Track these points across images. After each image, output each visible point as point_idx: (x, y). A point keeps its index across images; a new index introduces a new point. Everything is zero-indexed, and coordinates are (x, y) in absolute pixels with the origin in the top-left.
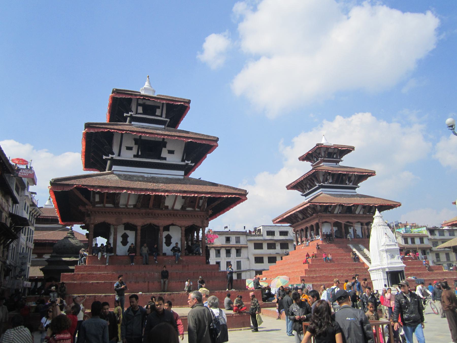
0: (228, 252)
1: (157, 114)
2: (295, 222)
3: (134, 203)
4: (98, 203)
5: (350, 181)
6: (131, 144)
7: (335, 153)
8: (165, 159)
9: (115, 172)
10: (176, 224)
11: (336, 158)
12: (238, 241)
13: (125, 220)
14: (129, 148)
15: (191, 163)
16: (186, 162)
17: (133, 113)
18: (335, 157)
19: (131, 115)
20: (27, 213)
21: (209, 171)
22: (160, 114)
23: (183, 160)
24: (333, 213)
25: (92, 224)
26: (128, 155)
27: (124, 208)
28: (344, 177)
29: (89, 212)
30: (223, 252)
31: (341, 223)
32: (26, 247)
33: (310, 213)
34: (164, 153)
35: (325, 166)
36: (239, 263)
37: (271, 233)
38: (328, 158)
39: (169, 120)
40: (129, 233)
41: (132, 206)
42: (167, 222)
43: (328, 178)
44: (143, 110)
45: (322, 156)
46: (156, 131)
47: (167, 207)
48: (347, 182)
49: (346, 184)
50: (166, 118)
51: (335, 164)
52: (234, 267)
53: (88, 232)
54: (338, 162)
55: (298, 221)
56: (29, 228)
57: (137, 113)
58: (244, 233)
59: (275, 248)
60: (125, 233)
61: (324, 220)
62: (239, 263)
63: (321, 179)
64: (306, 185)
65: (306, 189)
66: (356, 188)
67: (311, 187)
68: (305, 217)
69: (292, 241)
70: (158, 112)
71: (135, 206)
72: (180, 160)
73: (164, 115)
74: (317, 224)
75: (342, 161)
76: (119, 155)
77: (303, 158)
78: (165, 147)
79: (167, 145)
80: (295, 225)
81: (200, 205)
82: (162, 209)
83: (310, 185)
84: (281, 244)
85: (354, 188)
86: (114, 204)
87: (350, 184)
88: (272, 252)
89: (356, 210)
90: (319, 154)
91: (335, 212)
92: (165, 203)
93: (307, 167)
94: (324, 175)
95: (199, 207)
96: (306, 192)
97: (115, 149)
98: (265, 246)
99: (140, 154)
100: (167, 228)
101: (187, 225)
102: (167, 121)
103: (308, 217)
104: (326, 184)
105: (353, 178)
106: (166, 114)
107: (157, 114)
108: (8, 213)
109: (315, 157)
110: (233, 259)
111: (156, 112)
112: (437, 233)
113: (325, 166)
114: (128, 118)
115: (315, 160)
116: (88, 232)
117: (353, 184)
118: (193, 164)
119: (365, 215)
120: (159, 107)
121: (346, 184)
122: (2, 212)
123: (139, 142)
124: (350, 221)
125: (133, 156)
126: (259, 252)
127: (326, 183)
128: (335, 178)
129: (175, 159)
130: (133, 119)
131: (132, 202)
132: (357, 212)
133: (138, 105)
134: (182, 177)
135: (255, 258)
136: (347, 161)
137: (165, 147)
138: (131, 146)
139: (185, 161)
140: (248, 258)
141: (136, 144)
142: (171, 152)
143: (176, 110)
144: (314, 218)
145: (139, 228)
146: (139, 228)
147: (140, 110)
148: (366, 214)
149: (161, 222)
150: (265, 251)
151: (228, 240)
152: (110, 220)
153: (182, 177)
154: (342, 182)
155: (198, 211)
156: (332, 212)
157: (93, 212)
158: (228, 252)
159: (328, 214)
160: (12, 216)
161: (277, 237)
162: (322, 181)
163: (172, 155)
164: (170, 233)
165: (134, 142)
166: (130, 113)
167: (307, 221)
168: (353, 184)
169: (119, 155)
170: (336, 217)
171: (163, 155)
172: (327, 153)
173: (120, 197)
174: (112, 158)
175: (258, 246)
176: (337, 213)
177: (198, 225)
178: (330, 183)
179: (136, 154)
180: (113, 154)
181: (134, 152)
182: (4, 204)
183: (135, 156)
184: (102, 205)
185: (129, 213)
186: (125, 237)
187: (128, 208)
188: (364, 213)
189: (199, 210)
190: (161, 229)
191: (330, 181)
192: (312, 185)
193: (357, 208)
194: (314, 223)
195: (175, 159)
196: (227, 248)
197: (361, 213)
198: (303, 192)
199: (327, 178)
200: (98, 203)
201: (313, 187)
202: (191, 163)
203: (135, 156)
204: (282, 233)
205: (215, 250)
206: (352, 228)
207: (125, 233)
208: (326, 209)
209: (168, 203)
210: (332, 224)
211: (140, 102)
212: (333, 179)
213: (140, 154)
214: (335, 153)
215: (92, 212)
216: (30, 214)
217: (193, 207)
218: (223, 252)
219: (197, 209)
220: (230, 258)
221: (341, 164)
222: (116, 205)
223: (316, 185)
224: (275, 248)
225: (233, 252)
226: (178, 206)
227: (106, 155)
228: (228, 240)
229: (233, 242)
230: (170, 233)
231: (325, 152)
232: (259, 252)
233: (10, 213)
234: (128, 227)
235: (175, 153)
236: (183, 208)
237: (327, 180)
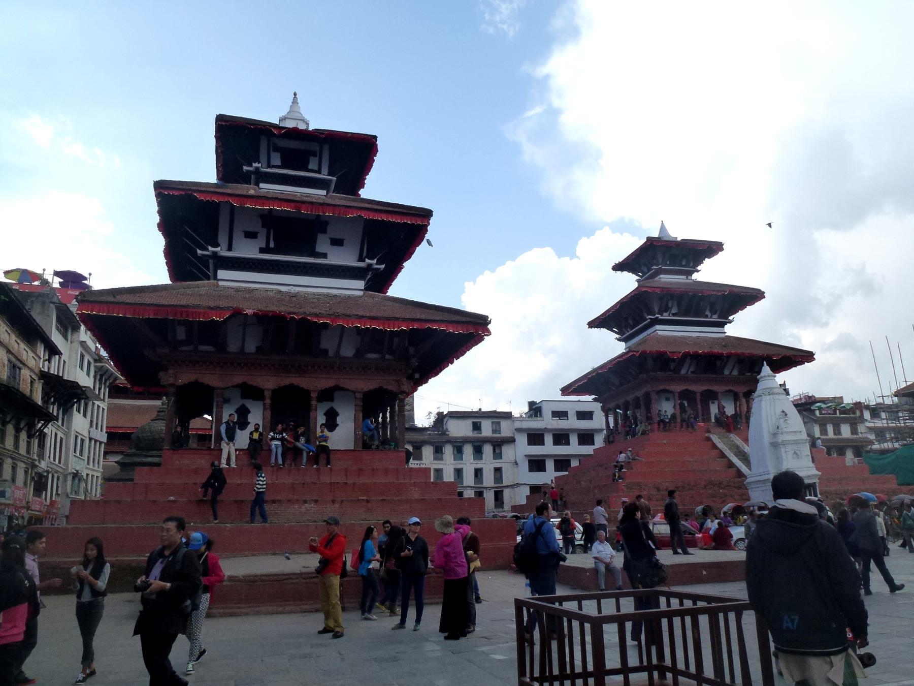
0: (478, 451)
1: (310, 167)
4: (182, 343)
5: (713, 312)
6: (256, 225)
8: (324, 256)
10: (346, 386)
12: (496, 429)
13: (238, 379)
15: (377, 264)
16: (367, 261)
19: (257, 168)
20: (88, 374)
21: (417, 282)
22: (316, 168)
23: (361, 259)
25: (172, 385)
26: (248, 250)
30: (468, 450)
31: (694, 393)
32: (91, 439)
34: (322, 245)
36: (498, 470)
37: (560, 414)
38: (669, 265)
39: (335, 179)
40: (249, 404)
42: (323, 383)
43: (670, 305)
47: (326, 352)
48: (708, 313)
50: (329, 174)
51: (685, 277)
52: (489, 479)
54: (691, 273)
56: (93, 404)
57: (269, 166)
58: (507, 416)
59: (568, 443)
61: (662, 387)
62: (498, 470)
64: (626, 319)
66: (726, 323)
67: (637, 323)
69: (601, 430)
71: (258, 349)
72: (356, 257)
73: (325, 170)
74: (647, 396)
75: (698, 271)
76: (230, 249)
77: (619, 267)
78: (324, 231)
79: (329, 229)
81: (394, 347)
85: (722, 325)
87: (715, 316)
88: (562, 450)
91: (683, 372)
92: (319, 343)
96: (628, 334)
97: (223, 239)
98: (549, 439)
99: (272, 245)
100: (327, 395)
101: (366, 389)
102: (330, 181)
104: (666, 316)
106: (330, 167)
107: (310, 167)
108: (37, 371)
110: (488, 463)
111: (308, 163)
114: (253, 176)
115: (645, 270)
117: (719, 318)
118: (383, 266)
120: (314, 155)
121: (707, 316)
122: (20, 369)
123: (270, 220)
124: (715, 388)
126: (536, 450)
127: (665, 314)
132: (726, 372)
134: (361, 293)
135: (530, 461)
136: (709, 272)
138: (256, 230)
139: (364, 261)
140: (516, 463)
142: (337, 242)
145: (267, 394)
146: (267, 394)
147: (276, 160)
148: (744, 374)
149: (315, 383)
150: (549, 448)
151: (477, 427)
152: (212, 379)
153: (361, 293)
155: (388, 360)
158: (478, 451)
160: (45, 377)
161: (572, 423)
162: (656, 309)
164: (337, 406)
166: (255, 165)
169: (230, 249)
170: (685, 379)
171: (320, 248)
175: (535, 438)
178: (674, 315)
179: (263, 245)
182: (25, 353)
183: (262, 251)
184: (190, 348)
188: (740, 373)
190: (314, 395)
191: (674, 311)
194: (640, 393)
196: (476, 444)
197: (735, 373)
199: (667, 304)
201: (639, 324)
202: (377, 264)
204: (585, 415)
205: (454, 447)
209: (327, 343)
210: (677, 395)
212: (679, 307)
213: (272, 245)
216: (95, 377)
218: (468, 450)
219: (387, 356)
220: (483, 461)
221: (696, 277)
222: (221, 347)
224: (568, 443)
225: (488, 449)
226: (348, 351)
228: (477, 427)
229: (487, 429)
232: (536, 450)
233: (41, 371)
236: (359, 353)
237: (667, 309)
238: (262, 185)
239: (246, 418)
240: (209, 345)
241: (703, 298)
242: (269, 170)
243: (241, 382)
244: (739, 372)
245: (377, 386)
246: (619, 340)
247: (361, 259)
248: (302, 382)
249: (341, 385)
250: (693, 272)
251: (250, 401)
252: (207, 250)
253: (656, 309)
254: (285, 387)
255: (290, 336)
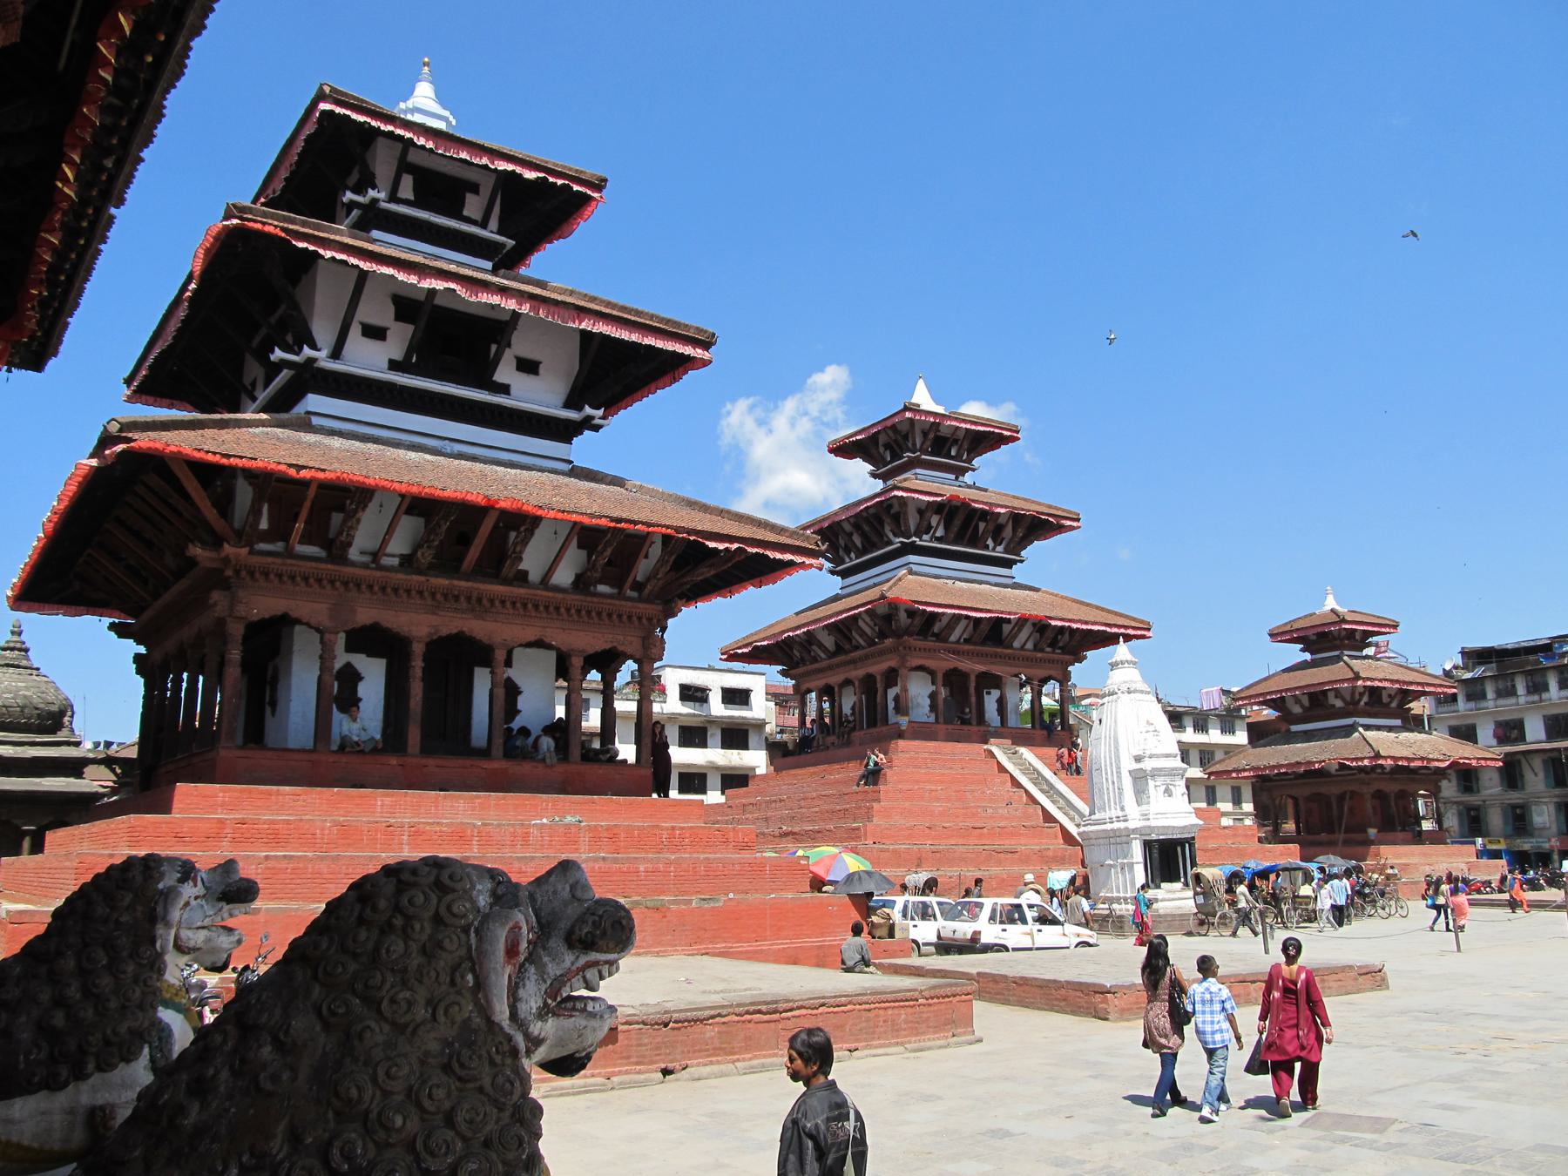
1: (465, 213)
2: (803, 660)
3: (405, 551)
5: (997, 542)
7: (955, 441)
8: (504, 389)
9: (315, 421)
11: (958, 458)
13: (366, 614)
14: (375, 333)
16: (588, 410)
17: (382, 195)
18: (953, 453)
19: (375, 201)
22: (477, 216)
23: (572, 402)
24: (945, 640)
26: (367, 359)
27: (365, 566)
28: (982, 526)
29: (229, 573)
33: (868, 630)
35: (926, 484)
40: (361, 662)
41: (396, 561)
43: (934, 524)
44: (417, 189)
45: (914, 444)
46: (451, 276)
47: (522, 577)
48: (990, 542)
49: (987, 547)
50: (499, 233)
53: (142, 650)
55: (815, 660)
57: (393, 198)
59: (703, 744)
60: (349, 665)
61: (917, 662)
63: (913, 522)
65: (848, 552)
66: (1015, 562)
67: (869, 546)
68: (847, 647)
70: (473, 206)
71: (407, 561)
73: (494, 223)
76: (336, 354)
80: (801, 670)
82: (506, 582)
83: (864, 535)
84: (724, 731)
86: (327, 544)
87: (1000, 548)
89: (1015, 637)
90: (906, 437)
91: (953, 638)
92: (521, 559)
93: (858, 482)
94: (921, 512)
95: (638, 587)
97: (324, 332)
102: (503, 245)
103: (857, 648)
105: (1008, 532)
106: (501, 220)
107: (465, 213)
109: (887, 446)
112: (1188, 721)
113: (926, 484)
116: (142, 650)
117: (1006, 551)
119: (1039, 655)
120: (474, 188)
121: (987, 547)
125: (386, 365)
127: (925, 537)
128: (957, 522)
129: (540, 394)
130: (373, 218)
131: (399, 545)
132: (1016, 644)
133: (404, 167)
137: (509, 345)
141: (400, 317)
142: (528, 366)
143: (541, 208)
144: (882, 653)
145: (418, 649)
146: (418, 649)
147: (407, 189)
148: (1042, 651)
154: (975, 541)
155: (630, 599)
156: (941, 637)
157: (243, 573)
159: (930, 643)
161: (717, 707)
162: (913, 528)
163: (532, 377)
165: (391, 310)
166: (372, 193)
167: (853, 662)
168: (1006, 551)
169: (336, 354)
172: (931, 436)
173: (358, 521)
174: (311, 361)
176: (958, 642)
177: (629, 650)
178: (939, 540)
179: (398, 355)
180: (314, 347)
181: (394, 347)
183: (394, 366)
184: (279, 546)
185: (383, 589)
186: (350, 678)
187: (381, 568)
188: (1036, 648)
189: (635, 594)
190: (500, 655)
192: (875, 539)
193: (1020, 630)
194: (878, 668)
195: (540, 394)
197: (1030, 646)
198: (837, 561)
200: (267, 537)
201: (875, 547)
203: (394, 366)
204: (737, 697)
206: (996, 694)
207: (349, 665)
208: (925, 624)
209: (533, 559)
210: (940, 676)
211: (413, 157)
212: (946, 528)
214: (955, 441)
215: (237, 572)
217: (618, 582)
219: (630, 593)
221: (968, 478)
222: (336, 550)
223: (890, 543)
226: (564, 576)
227: (287, 349)
230: (512, 673)
231: (925, 434)
234: (368, 640)
235: (542, 369)
236: (582, 583)
237: (928, 529)
238: (376, 234)
239: (355, 691)
240: (310, 543)
241: (984, 515)
242: (393, 207)
243: (368, 622)
244: (1035, 645)
245: (607, 646)
246: (833, 572)
247: (568, 404)
248: (478, 628)
249: (547, 640)
250: (966, 470)
251: (363, 656)
252: (297, 354)
253: (913, 528)
254: (450, 638)
255: (471, 538)
